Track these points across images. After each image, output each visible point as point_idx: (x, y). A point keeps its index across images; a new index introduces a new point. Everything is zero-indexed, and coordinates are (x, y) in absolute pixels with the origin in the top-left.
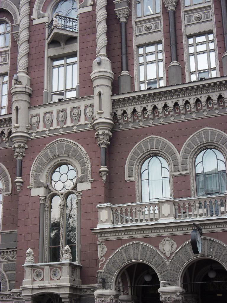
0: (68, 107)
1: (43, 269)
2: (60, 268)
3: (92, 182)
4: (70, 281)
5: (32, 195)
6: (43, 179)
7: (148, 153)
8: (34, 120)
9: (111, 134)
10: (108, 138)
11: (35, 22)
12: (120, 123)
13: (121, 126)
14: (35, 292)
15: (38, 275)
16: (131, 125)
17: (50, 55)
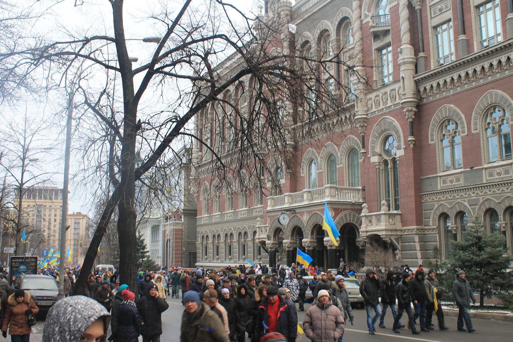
0: (388, 89)
1: (372, 218)
2: (380, 217)
3: (405, 149)
4: (386, 225)
5: (372, 161)
6: (378, 150)
7: (489, 107)
8: (370, 102)
9: (414, 109)
10: (413, 113)
11: (364, 22)
12: (424, 98)
13: (425, 100)
14: (369, 234)
15: (370, 222)
16: (431, 98)
17: (375, 48)
